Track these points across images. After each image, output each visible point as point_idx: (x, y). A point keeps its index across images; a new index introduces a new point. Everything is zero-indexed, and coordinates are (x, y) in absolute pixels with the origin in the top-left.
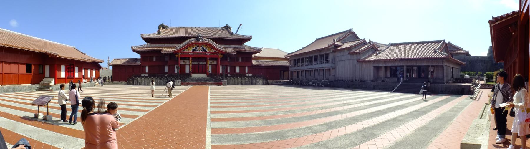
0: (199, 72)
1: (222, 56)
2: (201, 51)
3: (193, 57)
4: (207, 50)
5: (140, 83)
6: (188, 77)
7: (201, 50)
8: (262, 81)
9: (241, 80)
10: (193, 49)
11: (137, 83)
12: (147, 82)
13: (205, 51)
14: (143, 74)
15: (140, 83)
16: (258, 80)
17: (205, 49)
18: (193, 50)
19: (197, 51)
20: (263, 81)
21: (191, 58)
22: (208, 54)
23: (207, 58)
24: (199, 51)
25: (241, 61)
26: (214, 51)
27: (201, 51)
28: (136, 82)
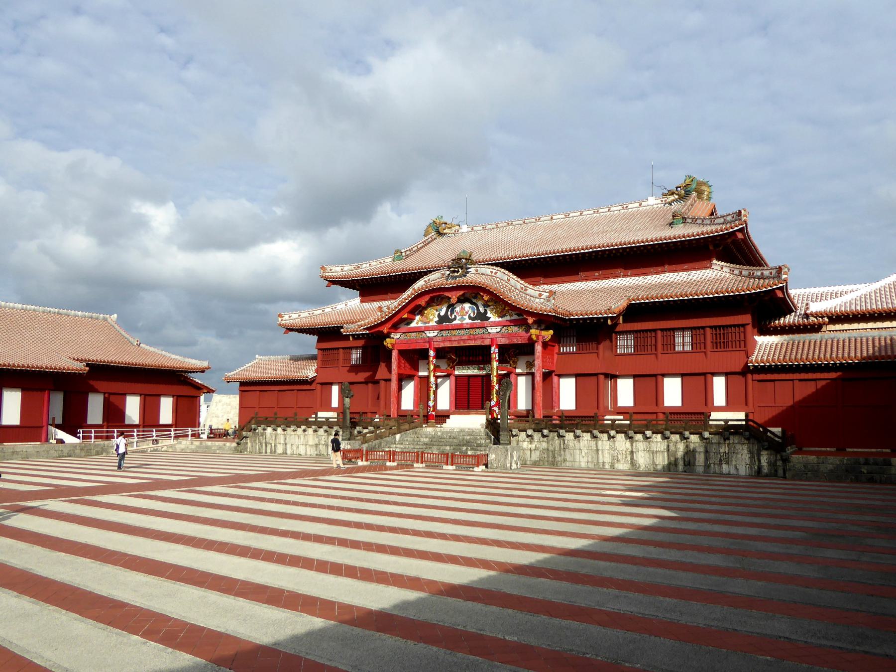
0: (468, 408)
1: (551, 332)
2: (467, 321)
3: (436, 345)
4: (489, 314)
5: (273, 445)
6: (406, 426)
7: (467, 317)
8: (750, 452)
9: (628, 444)
10: (439, 315)
11: (264, 445)
12: (292, 445)
13: (483, 317)
14: (322, 415)
15: (273, 445)
16: (724, 449)
17: (482, 309)
18: (442, 319)
19: (454, 322)
20: (755, 456)
21: (432, 353)
22: (493, 330)
23: (489, 347)
24: (462, 319)
25: (688, 348)
26: (518, 315)
27: (470, 318)
28: (261, 444)
